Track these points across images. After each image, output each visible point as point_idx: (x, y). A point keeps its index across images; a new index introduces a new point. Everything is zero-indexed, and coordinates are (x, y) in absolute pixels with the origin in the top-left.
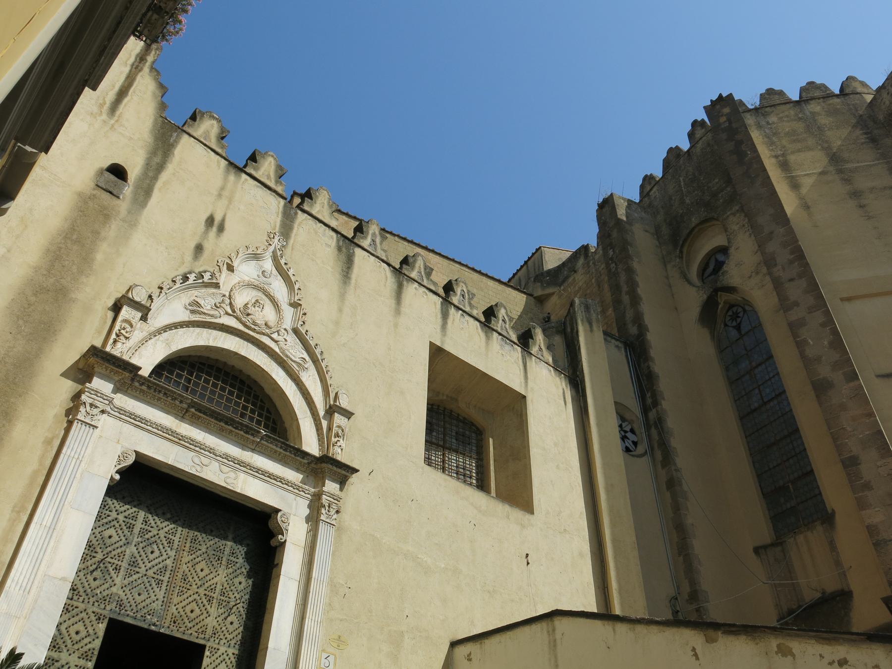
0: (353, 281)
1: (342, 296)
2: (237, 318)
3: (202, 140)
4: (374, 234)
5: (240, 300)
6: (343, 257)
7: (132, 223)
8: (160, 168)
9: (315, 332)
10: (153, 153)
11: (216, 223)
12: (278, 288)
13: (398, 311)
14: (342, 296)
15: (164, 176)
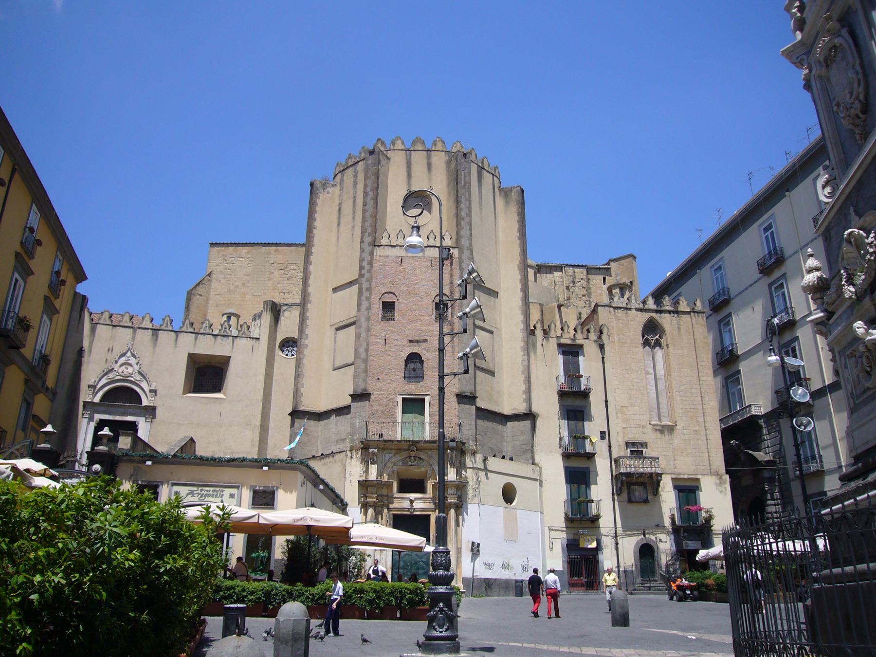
0: (158, 344)
1: (154, 352)
2: (120, 375)
3: (104, 323)
4: (167, 321)
5: (120, 371)
6: (155, 337)
7: (89, 362)
8: (93, 340)
9: (144, 370)
10: (90, 337)
11: (110, 351)
12: (133, 361)
13: (176, 347)
14: (154, 352)
15: (95, 342)
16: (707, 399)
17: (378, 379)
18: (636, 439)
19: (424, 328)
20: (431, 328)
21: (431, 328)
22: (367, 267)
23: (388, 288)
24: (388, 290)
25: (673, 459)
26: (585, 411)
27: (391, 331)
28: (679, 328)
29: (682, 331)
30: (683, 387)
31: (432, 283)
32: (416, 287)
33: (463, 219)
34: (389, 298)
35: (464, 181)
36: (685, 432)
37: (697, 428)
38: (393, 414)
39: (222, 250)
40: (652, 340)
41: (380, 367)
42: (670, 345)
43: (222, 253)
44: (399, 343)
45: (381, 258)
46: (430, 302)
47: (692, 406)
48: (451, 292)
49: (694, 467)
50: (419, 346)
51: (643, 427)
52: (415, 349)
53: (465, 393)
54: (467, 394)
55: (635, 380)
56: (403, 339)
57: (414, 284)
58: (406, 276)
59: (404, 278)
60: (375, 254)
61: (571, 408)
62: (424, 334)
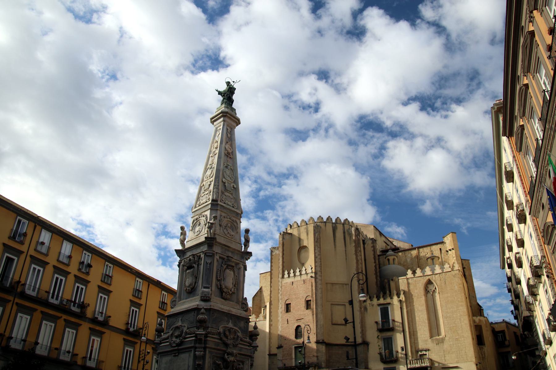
16: (462, 319)
17: (285, 339)
18: (422, 348)
19: (302, 313)
20: (305, 313)
21: (305, 313)
22: (280, 289)
23: (288, 297)
24: (288, 298)
25: (444, 356)
26: (392, 338)
27: (290, 317)
28: (445, 282)
29: (447, 283)
30: (448, 315)
31: (304, 291)
32: (298, 294)
33: (317, 257)
34: (287, 303)
35: (317, 238)
36: (450, 340)
37: (457, 337)
38: (291, 354)
39: (265, 276)
40: (431, 291)
41: (286, 334)
42: (440, 293)
43: (264, 277)
44: (293, 322)
45: (285, 284)
46: (304, 300)
47: (454, 325)
48: (312, 294)
49: (457, 360)
50: (300, 322)
51: (426, 341)
52: (298, 324)
53: (319, 341)
54: (320, 341)
55: (421, 316)
56: (294, 320)
57: (298, 294)
58: (295, 291)
59: (294, 291)
60: (282, 283)
61: (385, 337)
62: (301, 316)
